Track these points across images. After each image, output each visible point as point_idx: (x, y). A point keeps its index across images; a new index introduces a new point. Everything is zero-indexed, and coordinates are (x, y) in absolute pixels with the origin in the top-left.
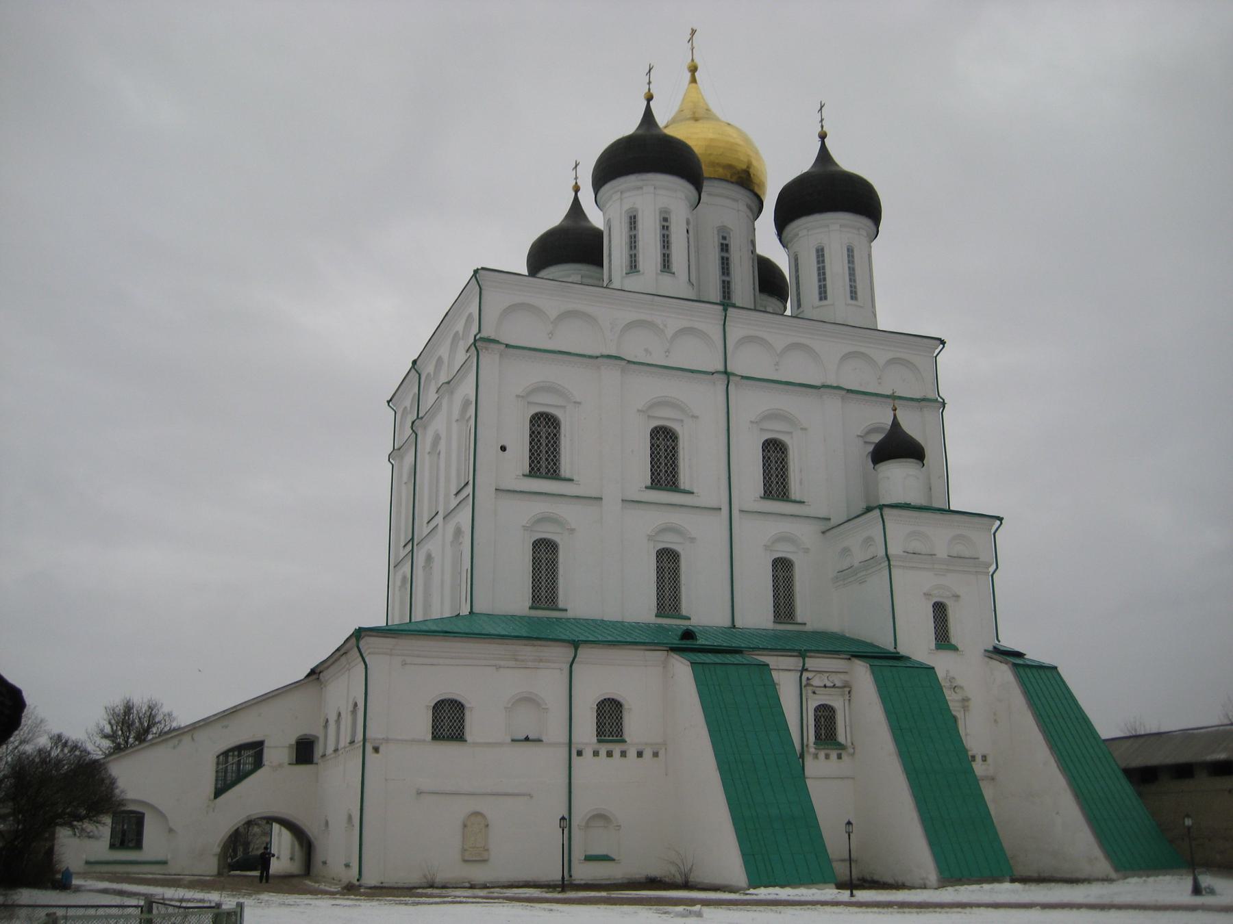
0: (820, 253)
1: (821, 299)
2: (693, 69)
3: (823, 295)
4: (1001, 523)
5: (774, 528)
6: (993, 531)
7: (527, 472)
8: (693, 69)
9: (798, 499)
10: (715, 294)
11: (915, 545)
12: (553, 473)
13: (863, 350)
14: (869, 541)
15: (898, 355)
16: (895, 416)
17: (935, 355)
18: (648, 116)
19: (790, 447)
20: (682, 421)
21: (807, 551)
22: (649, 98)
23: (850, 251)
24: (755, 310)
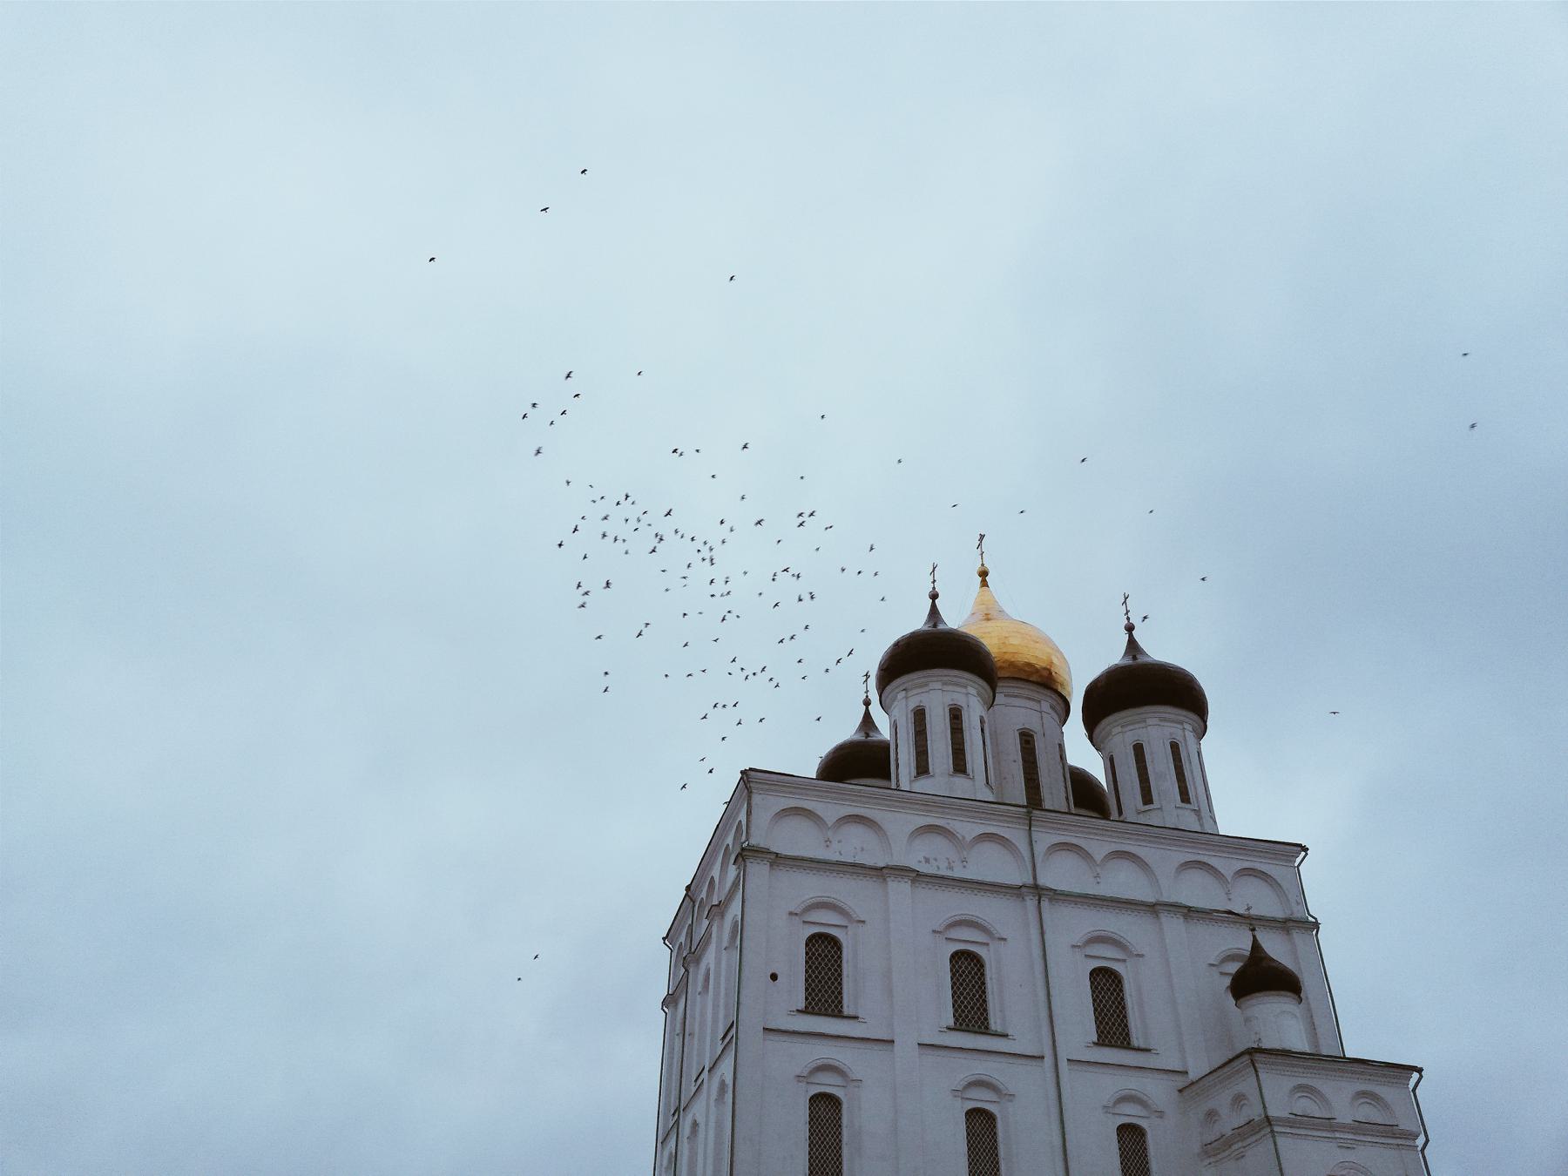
0: (1139, 750)
1: (1145, 803)
2: (984, 574)
3: (1147, 798)
4: (1421, 1077)
5: (1112, 1084)
6: (1411, 1086)
7: (802, 1005)
8: (984, 574)
9: (1142, 1046)
10: (1018, 793)
11: (1305, 1106)
12: (836, 1012)
13: (1205, 859)
14: (1239, 1100)
15: (1247, 865)
16: (1254, 937)
17: (1296, 864)
18: (934, 613)
19: (1125, 977)
20: (987, 944)
21: (1161, 1115)
22: (934, 596)
23: (1175, 747)
24: (1069, 813)
